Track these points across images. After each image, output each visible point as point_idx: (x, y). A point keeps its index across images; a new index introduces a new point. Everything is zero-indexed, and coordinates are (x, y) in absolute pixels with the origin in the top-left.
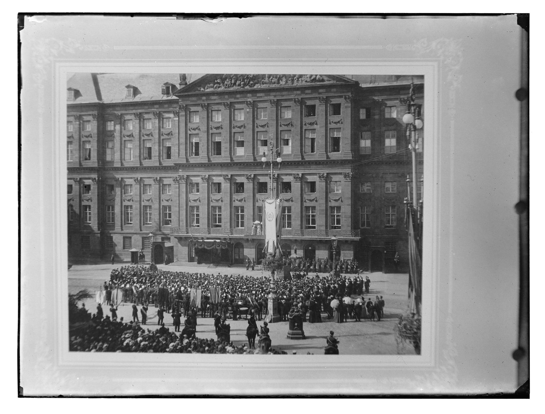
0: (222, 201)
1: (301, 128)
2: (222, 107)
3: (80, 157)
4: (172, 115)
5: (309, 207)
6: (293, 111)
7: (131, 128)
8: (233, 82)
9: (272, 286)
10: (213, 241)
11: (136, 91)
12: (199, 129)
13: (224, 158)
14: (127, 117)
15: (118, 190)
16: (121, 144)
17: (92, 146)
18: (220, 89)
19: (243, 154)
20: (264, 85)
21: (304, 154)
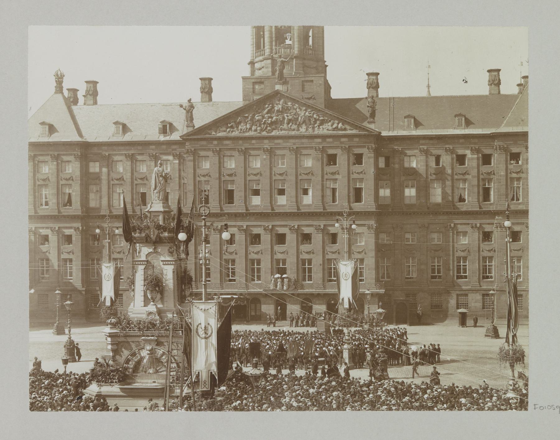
0: (236, 254)
1: (323, 177)
2: (236, 153)
3: (58, 203)
5: (331, 259)
7: (121, 170)
8: (248, 126)
9: (347, 338)
10: (230, 296)
11: (125, 129)
12: (210, 176)
13: (238, 206)
14: (116, 158)
15: (106, 242)
16: (109, 188)
17: (75, 191)
19: (259, 203)
20: (283, 132)
21: (326, 205)
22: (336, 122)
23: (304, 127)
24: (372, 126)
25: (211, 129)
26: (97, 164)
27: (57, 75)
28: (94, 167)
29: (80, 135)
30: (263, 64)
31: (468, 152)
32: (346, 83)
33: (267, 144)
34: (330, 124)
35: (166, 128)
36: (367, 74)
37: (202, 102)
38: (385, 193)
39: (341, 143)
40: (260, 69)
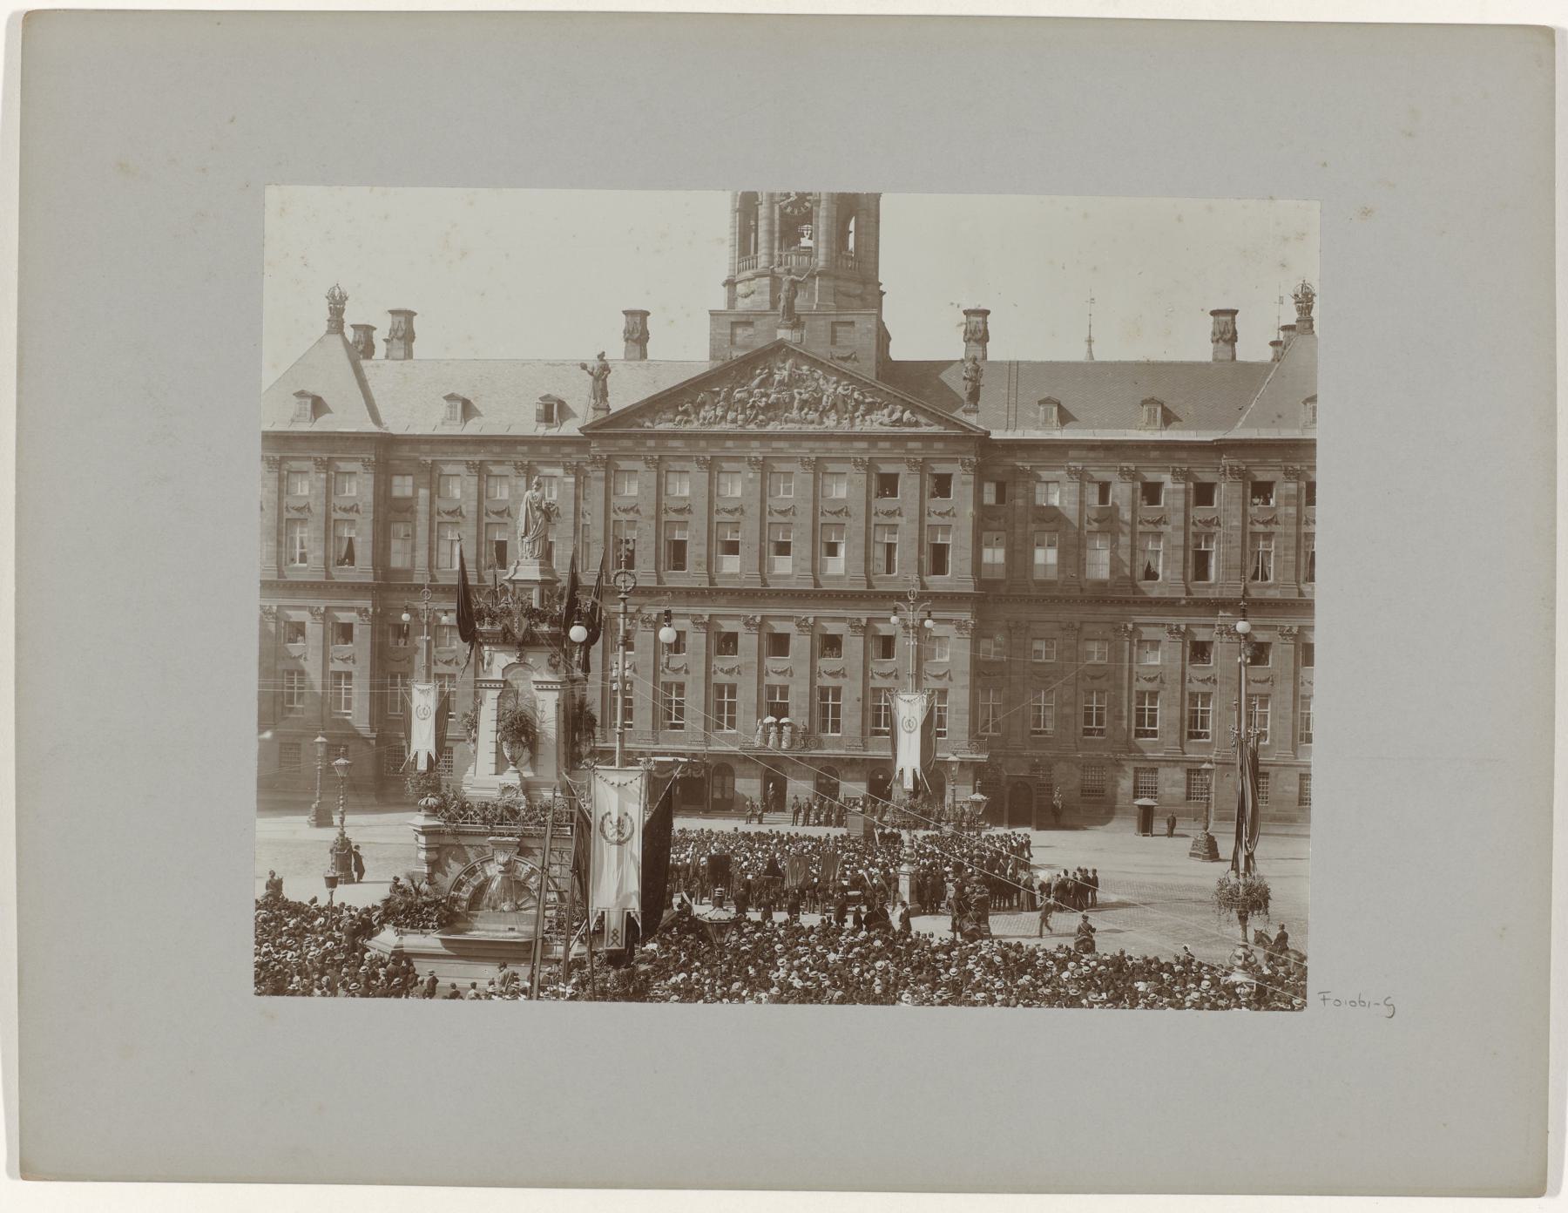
0: (687, 672)
1: (868, 521)
2: (692, 467)
3: (326, 558)
4: (559, 472)
5: (880, 690)
6: (850, 482)
7: (457, 493)
8: (719, 412)
9: (908, 851)
13: (692, 576)
14: (448, 469)
15: (422, 640)
16: (431, 530)
17: (362, 535)
18: (688, 428)
20: (790, 425)
21: (873, 578)
22: (900, 408)
23: (833, 416)
24: (972, 419)
25: (641, 416)
26: (409, 480)
27: (333, 297)
28: (402, 487)
29: (376, 420)
31: (1166, 478)
32: (920, 330)
33: (756, 450)
34: (886, 411)
35: (552, 410)
36: (966, 312)
37: (626, 359)
38: (994, 556)
39: (911, 451)
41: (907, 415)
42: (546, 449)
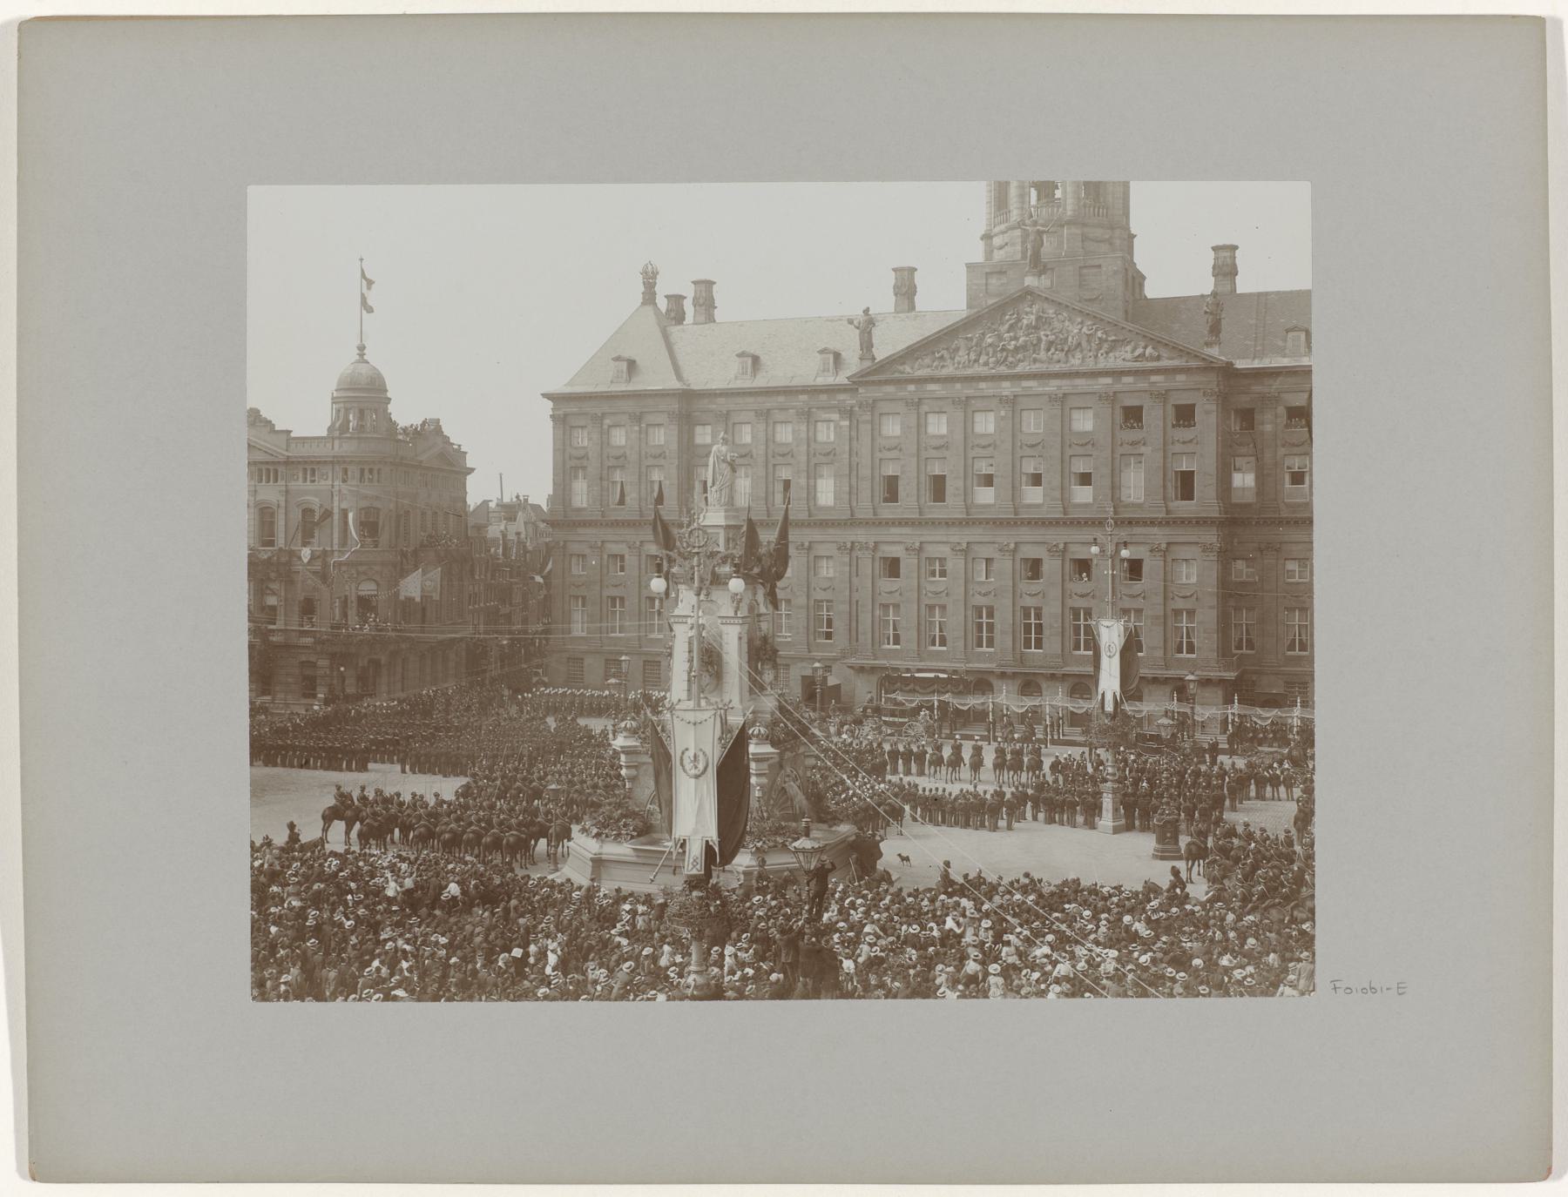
4: (836, 416)
6: (1096, 416)
7: (747, 439)
8: (973, 357)
10: (932, 675)
13: (953, 506)
23: (1078, 355)
24: (1214, 351)
26: (709, 429)
29: (679, 377)
30: (1006, 238)
32: (1172, 269)
33: (1007, 388)
34: (1129, 348)
36: (1214, 249)
37: (897, 312)
38: (1244, 480)
40: (1001, 248)
41: (1149, 350)
42: (824, 397)
